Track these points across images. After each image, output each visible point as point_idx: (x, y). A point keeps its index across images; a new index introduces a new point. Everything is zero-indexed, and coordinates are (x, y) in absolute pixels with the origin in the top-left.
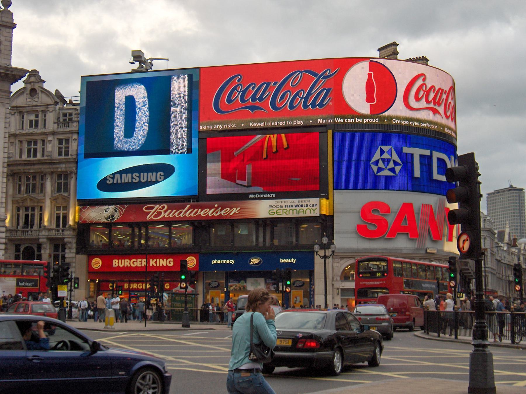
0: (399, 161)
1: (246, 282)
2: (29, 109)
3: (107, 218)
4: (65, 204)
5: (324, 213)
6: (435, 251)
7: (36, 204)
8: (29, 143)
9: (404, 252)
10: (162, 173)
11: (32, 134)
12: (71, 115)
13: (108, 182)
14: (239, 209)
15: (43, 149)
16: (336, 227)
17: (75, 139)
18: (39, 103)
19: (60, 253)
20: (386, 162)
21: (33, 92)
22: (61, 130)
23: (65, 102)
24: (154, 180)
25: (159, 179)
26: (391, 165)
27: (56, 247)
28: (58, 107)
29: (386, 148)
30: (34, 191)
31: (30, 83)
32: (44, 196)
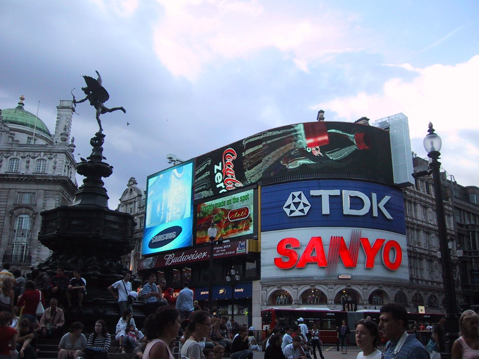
0: (308, 204)
1: (228, 308)
3: (149, 266)
5: (251, 251)
6: (350, 277)
9: (315, 279)
10: (175, 233)
13: (153, 242)
14: (206, 253)
16: (263, 261)
18: (132, 197)
20: (297, 204)
22: (141, 212)
24: (171, 238)
26: (301, 207)
29: (296, 194)
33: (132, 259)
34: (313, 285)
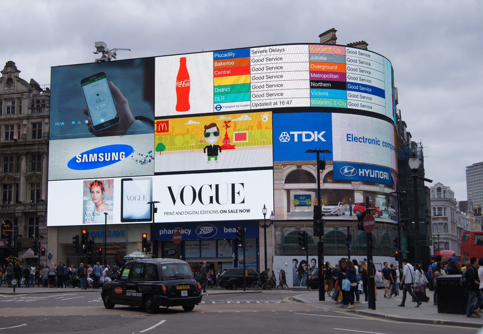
2: (6, 96)
4: (38, 181)
7: (13, 182)
8: (7, 127)
11: (9, 119)
12: (43, 101)
15: (19, 132)
17: (46, 123)
18: (15, 91)
19: (35, 226)
21: (10, 80)
23: (41, 90)
25: (121, 158)
27: (31, 221)
28: (32, 94)
30: (11, 171)
31: (7, 73)
32: (20, 175)
33: (23, 180)
34: (338, 227)
